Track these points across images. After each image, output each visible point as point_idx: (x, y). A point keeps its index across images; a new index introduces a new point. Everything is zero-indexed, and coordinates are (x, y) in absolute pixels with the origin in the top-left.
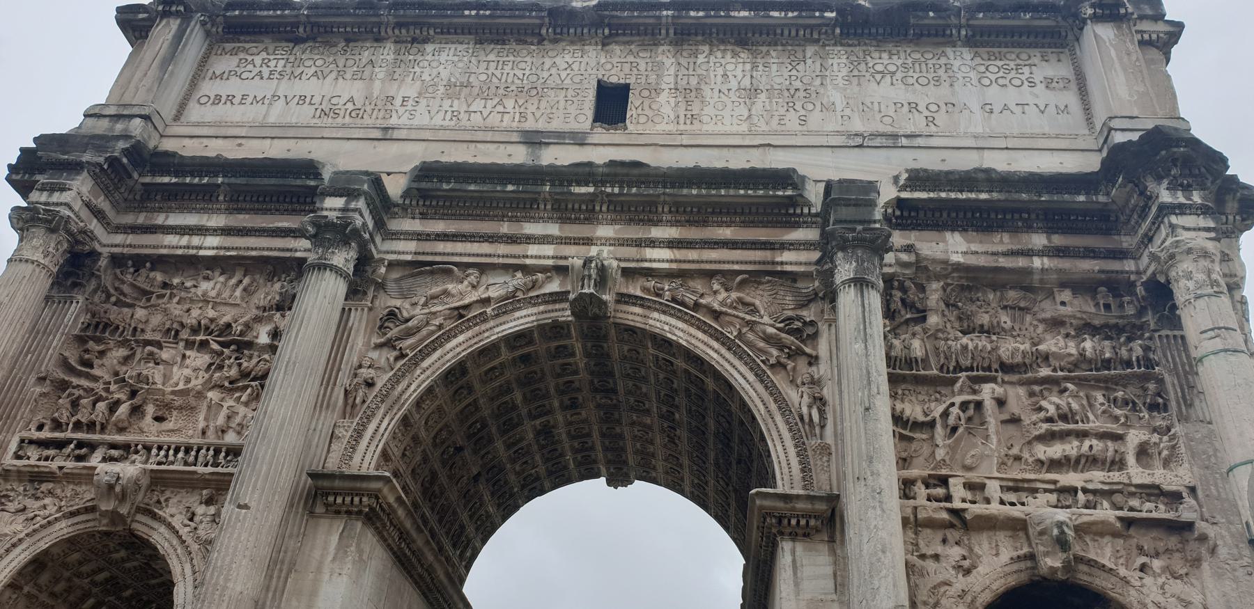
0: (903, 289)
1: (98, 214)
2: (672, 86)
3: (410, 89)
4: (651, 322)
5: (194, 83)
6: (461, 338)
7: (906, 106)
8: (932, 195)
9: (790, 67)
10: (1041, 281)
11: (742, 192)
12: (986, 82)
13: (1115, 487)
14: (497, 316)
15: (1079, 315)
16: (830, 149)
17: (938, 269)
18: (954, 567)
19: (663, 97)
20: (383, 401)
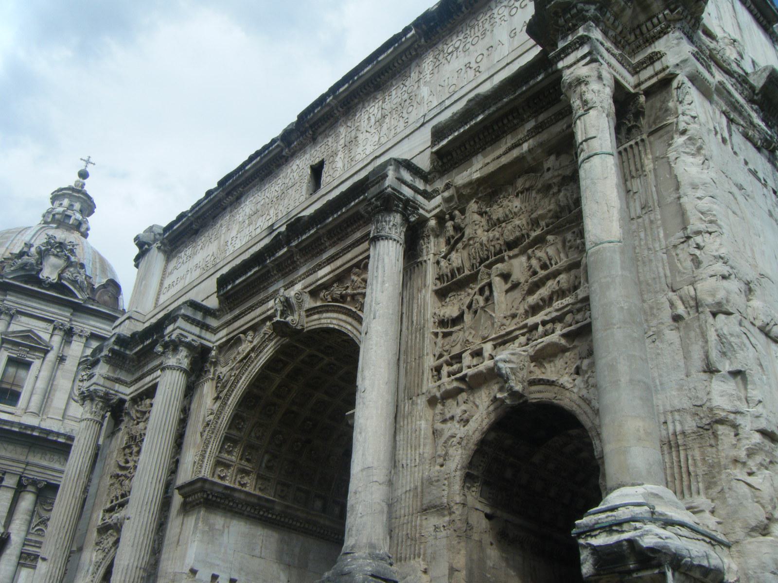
0: (452, 218)
1: (117, 380)
2: (343, 145)
3: (234, 233)
4: (323, 321)
5: (161, 284)
6: (243, 378)
7: (464, 68)
8: (450, 138)
9: (402, 86)
10: (534, 159)
11: (353, 204)
12: (514, 11)
13: (566, 309)
14: (257, 356)
15: (556, 173)
16: (407, 139)
17: (468, 191)
18: (458, 422)
19: (341, 155)
20: (213, 433)
